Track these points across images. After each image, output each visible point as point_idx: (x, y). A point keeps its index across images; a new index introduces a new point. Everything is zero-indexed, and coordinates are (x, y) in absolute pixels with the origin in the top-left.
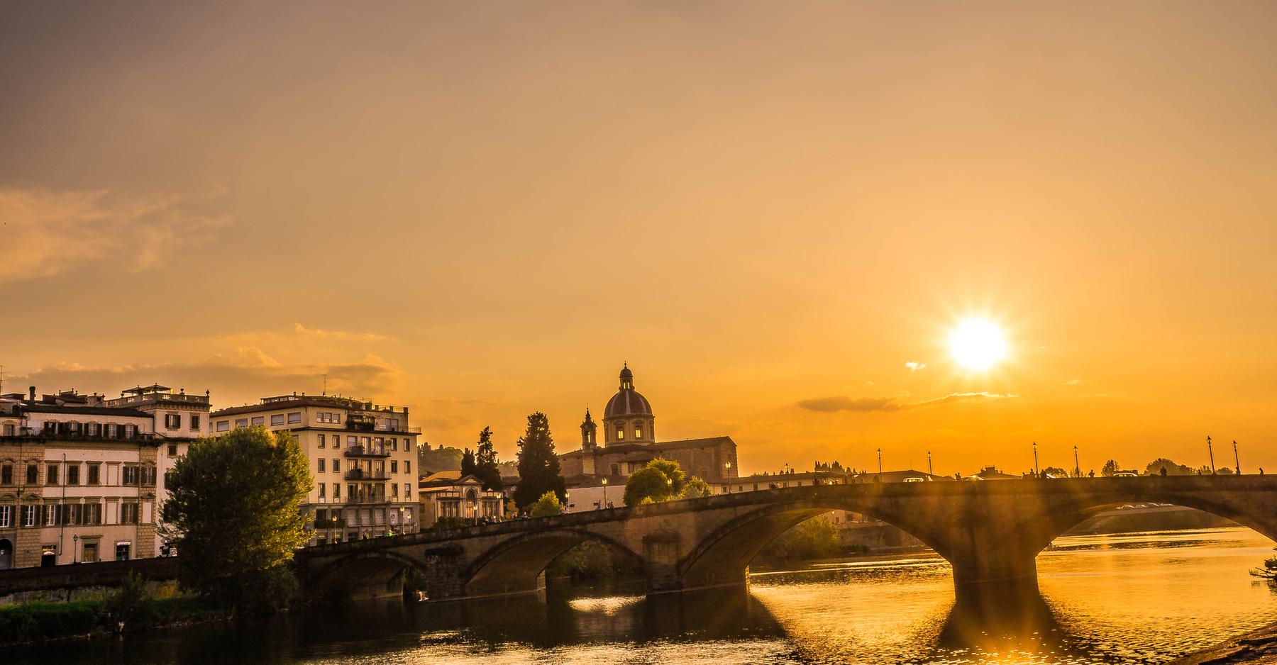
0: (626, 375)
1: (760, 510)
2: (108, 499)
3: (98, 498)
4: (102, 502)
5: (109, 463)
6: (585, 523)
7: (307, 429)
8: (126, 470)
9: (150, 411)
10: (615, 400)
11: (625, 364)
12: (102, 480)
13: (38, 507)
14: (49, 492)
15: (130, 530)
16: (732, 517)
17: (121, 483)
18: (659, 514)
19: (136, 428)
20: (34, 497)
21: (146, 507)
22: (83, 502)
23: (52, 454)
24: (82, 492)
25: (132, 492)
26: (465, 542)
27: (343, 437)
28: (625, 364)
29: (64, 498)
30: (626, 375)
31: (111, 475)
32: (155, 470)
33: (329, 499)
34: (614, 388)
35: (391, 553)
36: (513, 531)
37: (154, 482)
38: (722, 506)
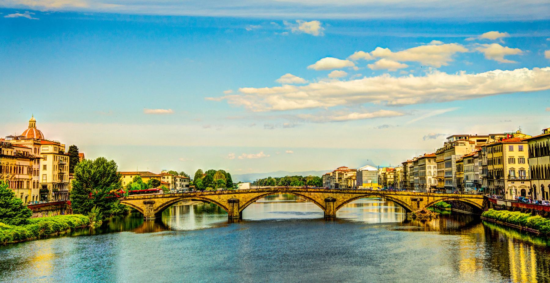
1: (267, 194)
2: (25, 179)
3: (23, 179)
4: (24, 180)
5: (26, 166)
6: (205, 195)
10: (27, 132)
12: (24, 174)
13: (12, 181)
16: (258, 195)
17: (27, 174)
18: (233, 194)
20: (15, 178)
21: (30, 182)
24: (21, 176)
26: (156, 200)
29: (19, 179)
35: (123, 202)
36: (176, 197)
38: (255, 192)
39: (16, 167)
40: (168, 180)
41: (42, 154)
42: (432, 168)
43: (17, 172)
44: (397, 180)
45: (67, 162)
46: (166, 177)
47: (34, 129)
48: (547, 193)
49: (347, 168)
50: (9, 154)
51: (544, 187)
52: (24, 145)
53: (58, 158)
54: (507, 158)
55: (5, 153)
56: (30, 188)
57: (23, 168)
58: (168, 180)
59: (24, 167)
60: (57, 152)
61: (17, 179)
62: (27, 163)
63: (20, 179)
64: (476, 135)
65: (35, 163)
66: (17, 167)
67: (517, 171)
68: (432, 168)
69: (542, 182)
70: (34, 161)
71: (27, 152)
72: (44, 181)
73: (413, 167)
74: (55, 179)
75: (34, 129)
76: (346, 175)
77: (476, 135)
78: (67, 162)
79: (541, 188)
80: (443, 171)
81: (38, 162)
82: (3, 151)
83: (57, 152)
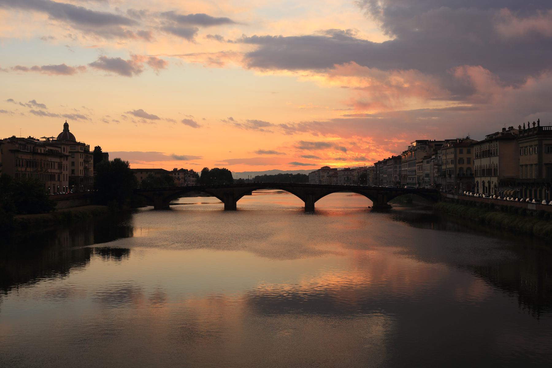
0: (66, 126)
2: (56, 173)
4: (55, 174)
5: (56, 162)
7: (78, 152)
8: (58, 164)
9: (60, 146)
10: (62, 135)
11: (66, 121)
14: (49, 171)
15: (59, 182)
19: (59, 151)
20: (48, 171)
22: (53, 174)
23: (50, 159)
24: (53, 171)
25: (58, 171)
27: (83, 154)
28: (66, 121)
29: (51, 172)
30: (66, 126)
31: (56, 165)
32: (62, 164)
33: (81, 175)
34: (61, 130)
37: (62, 168)
39: (48, 163)
40: (179, 176)
41: (69, 152)
42: (398, 167)
43: (49, 167)
44: (370, 177)
45: (92, 159)
46: (177, 174)
47: (67, 132)
48: (486, 188)
49: (329, 167)
50: (43, 152)
51: (484, 183)
52: (55, 145)
53: (84, 156)
54: (458, 159)
55: (39, 151)
56: (61, 180)
57: (54, 164)
58: (179, 176)
59: (55, 163)
60: (83, 151)
61: (49, 173)
62: (58, 160)
63: (52, 173)
64: (435, 140)
65: (64, 159)
66: (49, 163)
67: (465, 169)
68: (398, 167)
69: (483, 179)
70: (63, 158)
71: (57, 151)
72: (73, 175)
73: (383, 167)
74: (82, 173)
75: (67, 132)
76: (328, 173)
77: (435, 140)
78: (92, 159)
79: (482, 183)
80: (407, 170)
81: (67, 160)
82: (38, 149)
83: (83, 151)
